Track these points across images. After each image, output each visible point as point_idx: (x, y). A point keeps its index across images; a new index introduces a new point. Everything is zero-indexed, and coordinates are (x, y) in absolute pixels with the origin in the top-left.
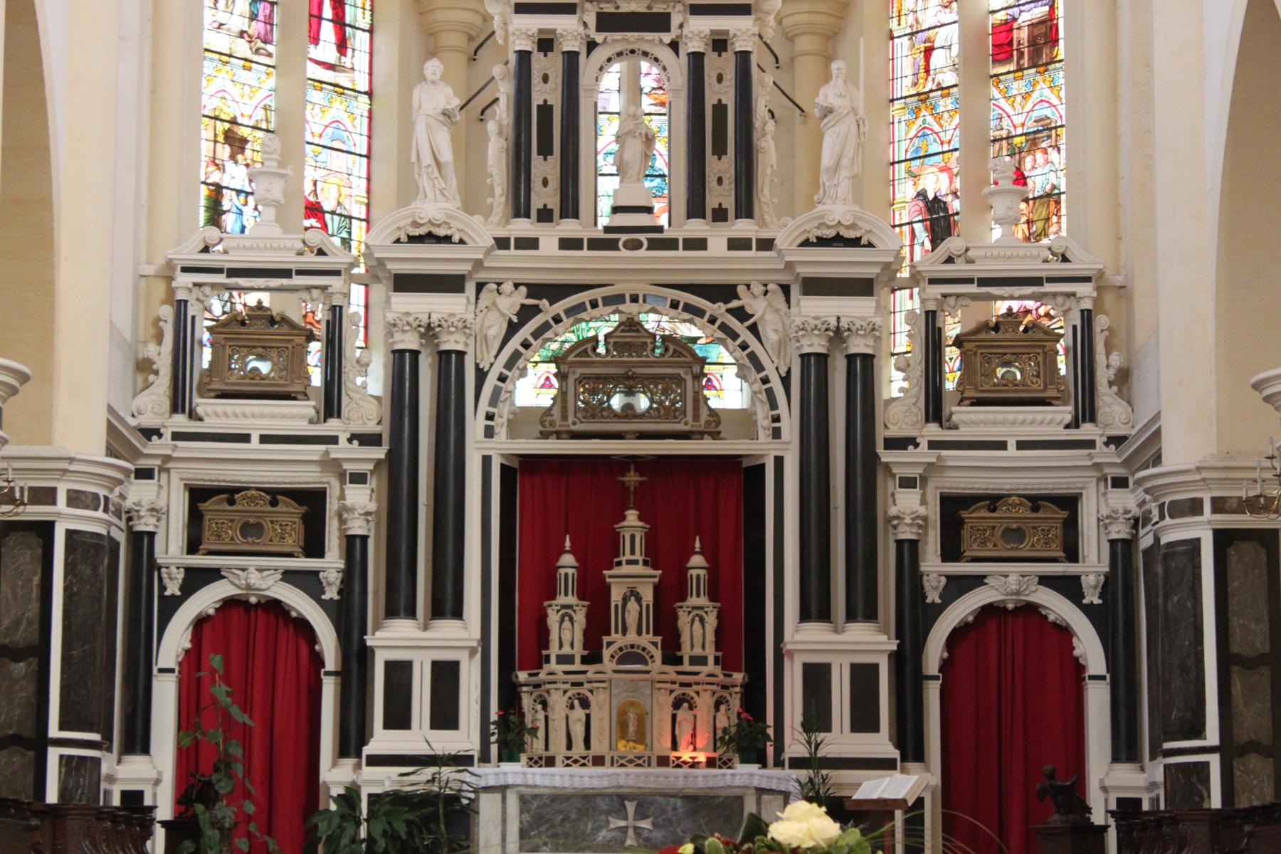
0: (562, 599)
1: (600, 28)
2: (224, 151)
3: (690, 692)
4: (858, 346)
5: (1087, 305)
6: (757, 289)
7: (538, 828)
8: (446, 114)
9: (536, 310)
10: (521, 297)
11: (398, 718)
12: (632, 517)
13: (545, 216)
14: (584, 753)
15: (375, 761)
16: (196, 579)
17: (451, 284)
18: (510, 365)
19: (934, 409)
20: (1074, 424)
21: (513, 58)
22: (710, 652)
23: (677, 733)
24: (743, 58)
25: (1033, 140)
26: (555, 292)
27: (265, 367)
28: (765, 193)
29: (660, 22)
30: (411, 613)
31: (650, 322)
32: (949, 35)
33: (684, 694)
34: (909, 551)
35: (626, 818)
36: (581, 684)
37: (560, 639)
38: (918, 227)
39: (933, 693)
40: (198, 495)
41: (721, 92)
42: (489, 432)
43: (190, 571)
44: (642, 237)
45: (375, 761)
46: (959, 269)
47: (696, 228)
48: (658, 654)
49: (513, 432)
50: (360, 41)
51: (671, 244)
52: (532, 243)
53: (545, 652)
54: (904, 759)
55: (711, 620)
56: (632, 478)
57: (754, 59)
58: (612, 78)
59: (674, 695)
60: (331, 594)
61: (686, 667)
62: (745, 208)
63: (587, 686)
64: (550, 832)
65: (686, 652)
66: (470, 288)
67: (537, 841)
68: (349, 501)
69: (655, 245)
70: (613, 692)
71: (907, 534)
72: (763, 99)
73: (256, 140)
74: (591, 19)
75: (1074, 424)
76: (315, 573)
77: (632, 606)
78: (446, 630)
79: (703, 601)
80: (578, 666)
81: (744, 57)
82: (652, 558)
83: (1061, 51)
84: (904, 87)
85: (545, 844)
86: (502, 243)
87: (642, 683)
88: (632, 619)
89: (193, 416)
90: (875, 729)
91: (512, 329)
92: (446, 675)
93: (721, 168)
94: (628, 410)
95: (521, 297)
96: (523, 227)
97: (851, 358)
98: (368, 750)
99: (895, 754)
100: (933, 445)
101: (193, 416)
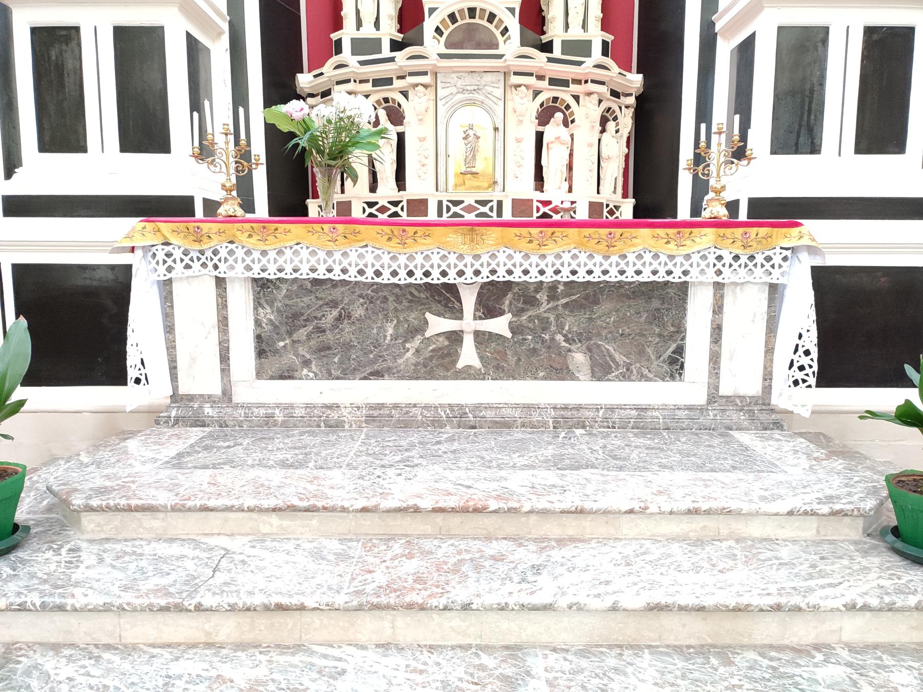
3: (565, 95)
7: (290, 334)
14: (395, 195)
22: (596, 36)
23: (544, 162)
33: (555, 99)
35: (457, 314)
36: (388, 81)
37: (358, 12)
53: (334, 36)
59: (541, 98)
63: (397, 84)
64: (312, 343)
67: (290, 358)
70: (441, 93)
85: (306, 363)
87: (489, 78)
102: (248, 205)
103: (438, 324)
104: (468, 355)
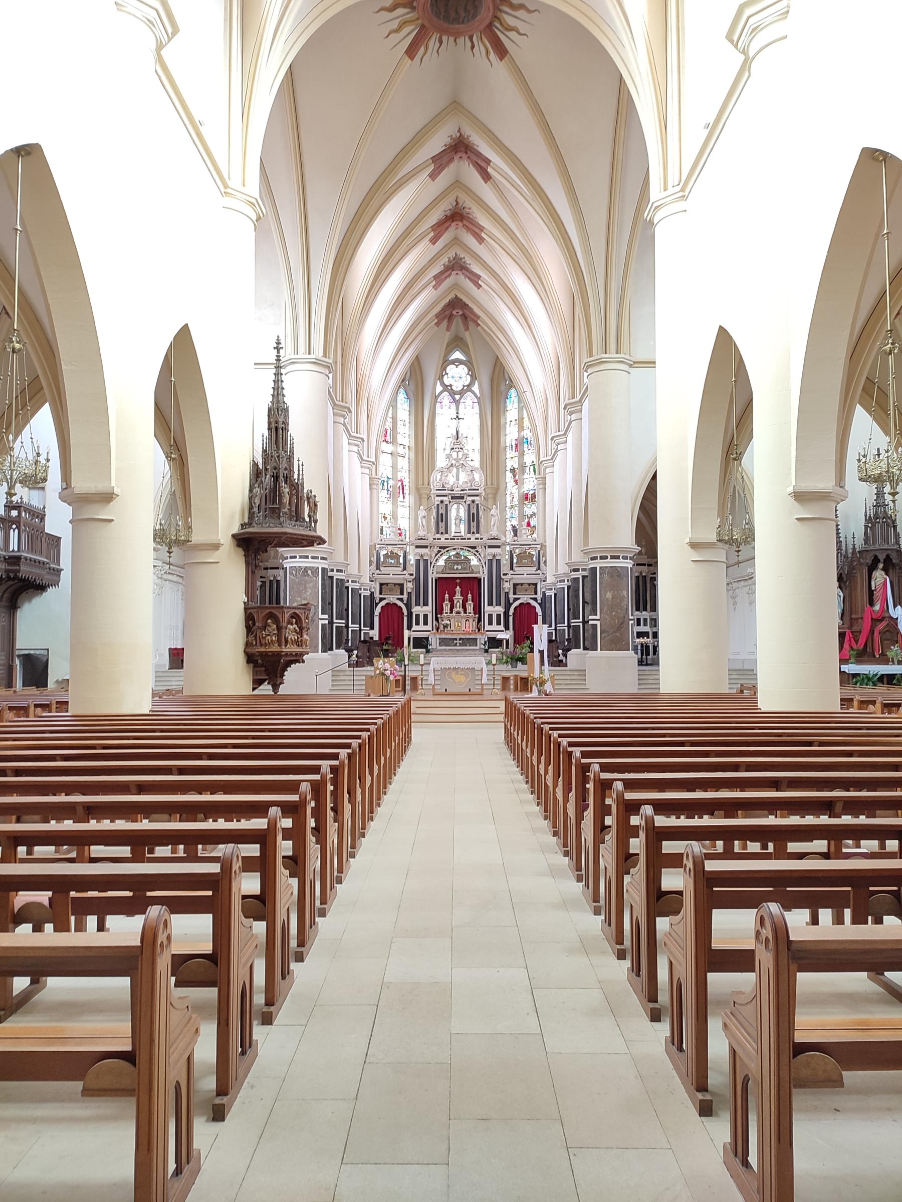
0: (446, 602)
1: (452, 499)
2: (383, 519)
4: (498, 558)
5: (539, 549)
6: (480, 547)
8: (424, 517)
9: (440, 551)
10: (438, 549)
11: (418, 623)
12: (458, 588)
13: (442, 533)
15: (413, 631)
16: (381, 599)
17: (426, 547)
18: (436, 561)
19: (512, 568)
20: (537, 570)
21: (436, 505)
22: (472, 612)
24: (478, 504)
25: (532, 516)
26: (444, 548)
27: (393, 561)
28: (481, 529)
29: (463, 498)
30: (420, 605)
31: (461, 553)
32: (516, 495)
34: (507, 594)
38: (511, 531)
39: (511, 619)
40: (381, 585)
41: (473, 510)
42: (433, 573)
43: (380, 598)
44: (460, 538)
45: (413, 631)
46: (516, 543)
47: (469, 536)
48: (463, 612)
49: (437, 573)
50: (407, 496)
51: (465, 539)
52: (440, 539)
54: (506, 630)
55: (472, 606)
56: (458, 581)
57: (480, 505)
58: (455, 506)
60: (405, 602)
61: (468, 614)
62: (478, 532)
65: (468, 612)
66: (429, 547)
68: (408, 585)
69: (461, 539)
71: (506, 591)
72: (481, 513)
73: (389, 517)
74: (450, 497)
75: (537, 570)
76: (402, 599)
77: (458, 603)
78: (425, 608)
79: (471, 602)
80: (449, 614)
81: (478, 504)
82: (462, 595)
83: (536, 499)
84: (508, 504)
86: (434, 539)
88: (458, 606)
89: (380, 570)
90: (500, 624)
91: (436, 555)
92: (426, 616)
93: (473, 524)
94: (457, 568)
95: (438, 549)
96: (438, 536)
97: (497, 560)
98: (412, 629)
99: (504, 629)
100: (511, 575)
101: (380, 570)
102: (433, 630)
103: (455, 642)
104: (458, 644)
